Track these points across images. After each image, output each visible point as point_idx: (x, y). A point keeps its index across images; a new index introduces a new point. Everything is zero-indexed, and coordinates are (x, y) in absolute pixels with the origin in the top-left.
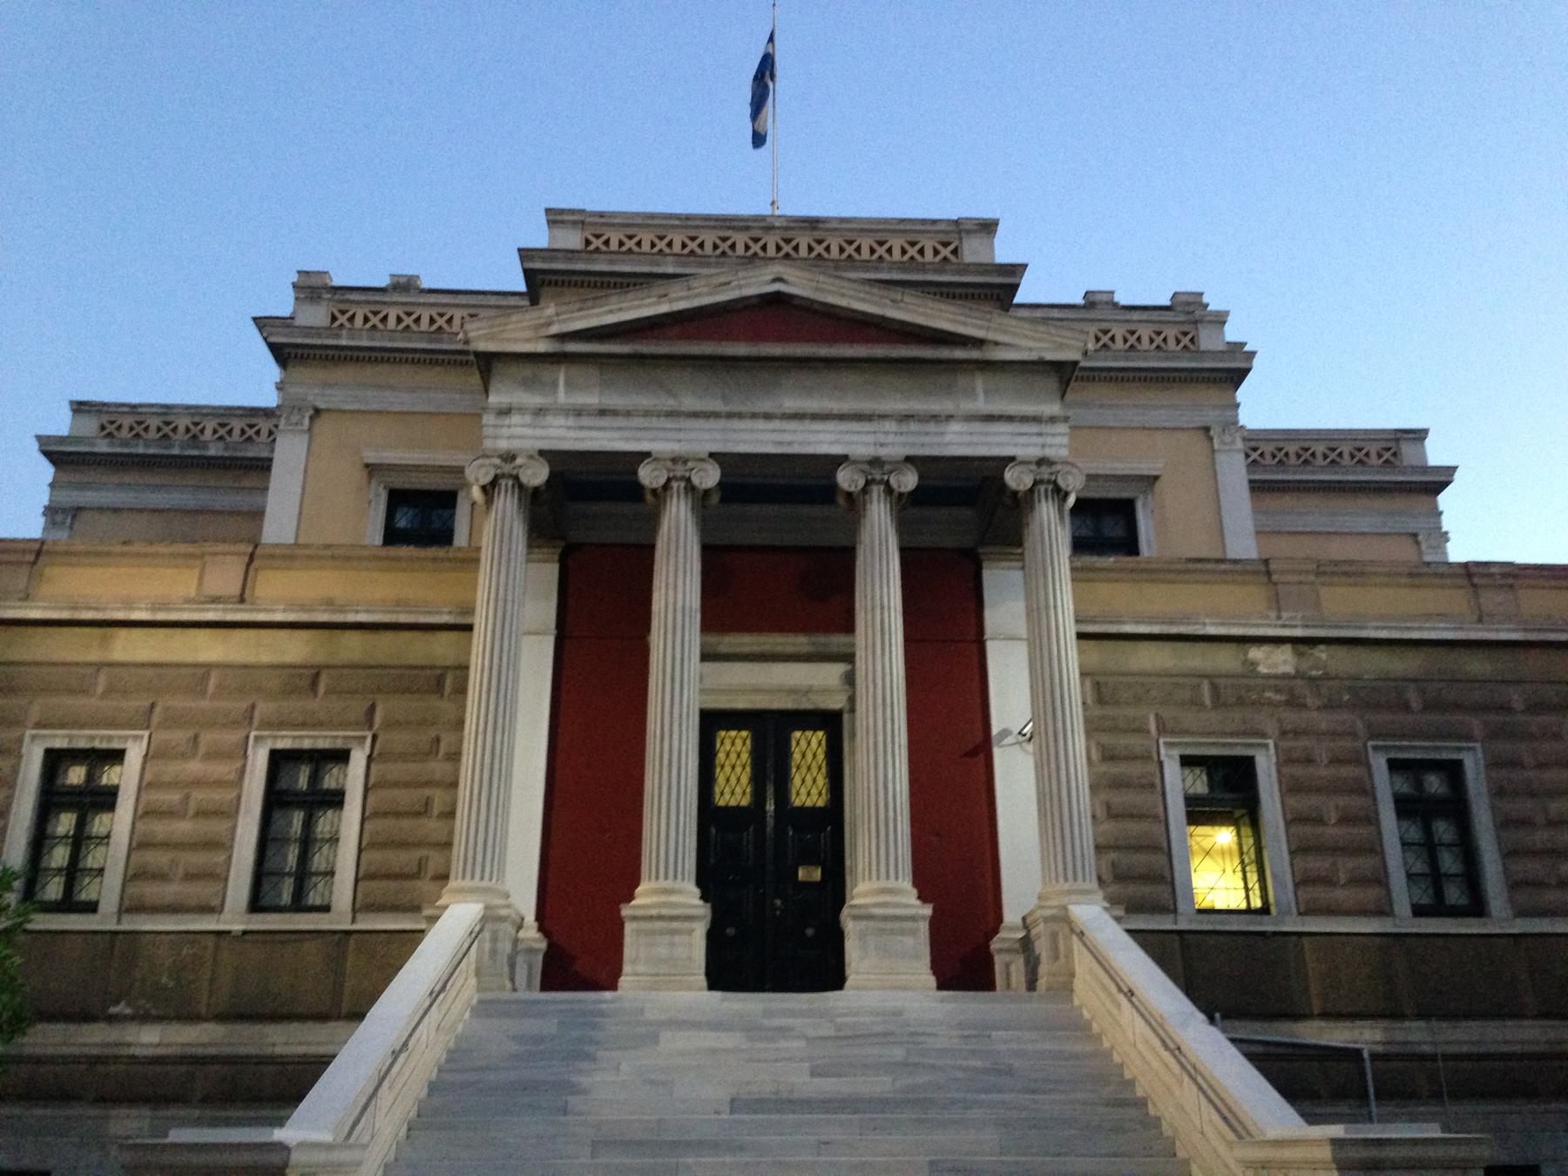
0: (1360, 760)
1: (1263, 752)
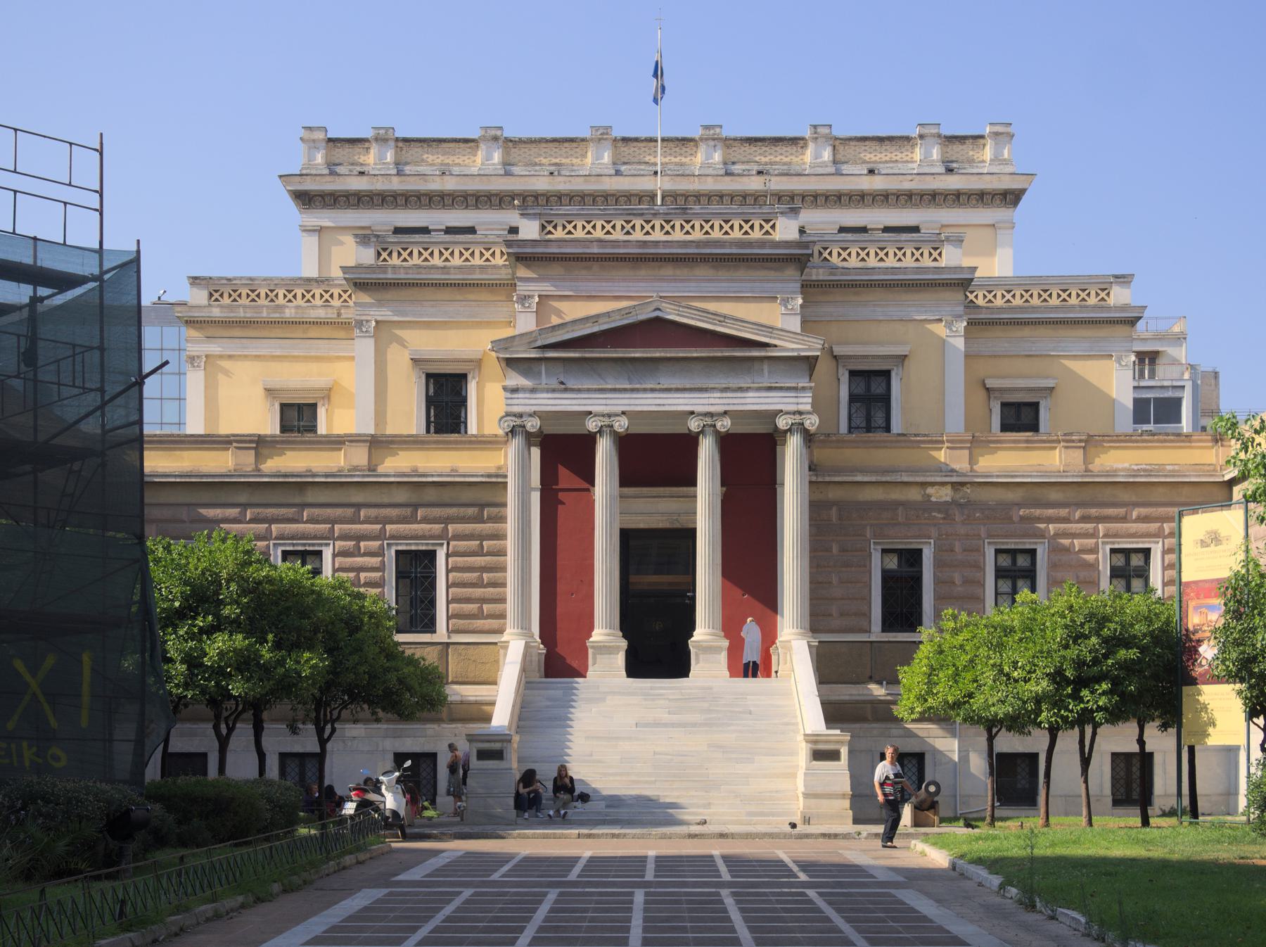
0: (980, 551)
1: (928, 546)
